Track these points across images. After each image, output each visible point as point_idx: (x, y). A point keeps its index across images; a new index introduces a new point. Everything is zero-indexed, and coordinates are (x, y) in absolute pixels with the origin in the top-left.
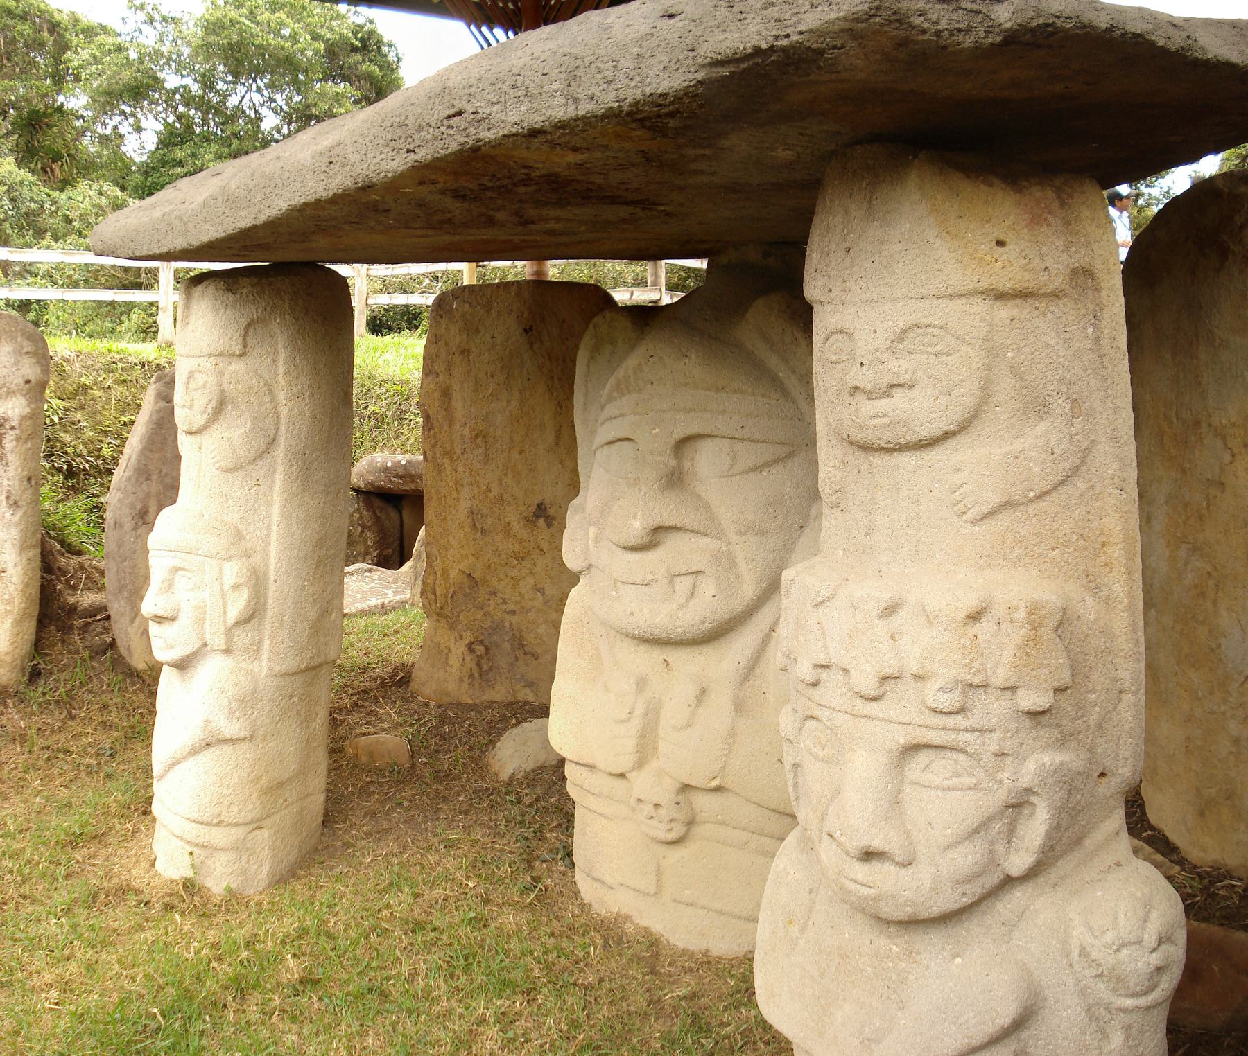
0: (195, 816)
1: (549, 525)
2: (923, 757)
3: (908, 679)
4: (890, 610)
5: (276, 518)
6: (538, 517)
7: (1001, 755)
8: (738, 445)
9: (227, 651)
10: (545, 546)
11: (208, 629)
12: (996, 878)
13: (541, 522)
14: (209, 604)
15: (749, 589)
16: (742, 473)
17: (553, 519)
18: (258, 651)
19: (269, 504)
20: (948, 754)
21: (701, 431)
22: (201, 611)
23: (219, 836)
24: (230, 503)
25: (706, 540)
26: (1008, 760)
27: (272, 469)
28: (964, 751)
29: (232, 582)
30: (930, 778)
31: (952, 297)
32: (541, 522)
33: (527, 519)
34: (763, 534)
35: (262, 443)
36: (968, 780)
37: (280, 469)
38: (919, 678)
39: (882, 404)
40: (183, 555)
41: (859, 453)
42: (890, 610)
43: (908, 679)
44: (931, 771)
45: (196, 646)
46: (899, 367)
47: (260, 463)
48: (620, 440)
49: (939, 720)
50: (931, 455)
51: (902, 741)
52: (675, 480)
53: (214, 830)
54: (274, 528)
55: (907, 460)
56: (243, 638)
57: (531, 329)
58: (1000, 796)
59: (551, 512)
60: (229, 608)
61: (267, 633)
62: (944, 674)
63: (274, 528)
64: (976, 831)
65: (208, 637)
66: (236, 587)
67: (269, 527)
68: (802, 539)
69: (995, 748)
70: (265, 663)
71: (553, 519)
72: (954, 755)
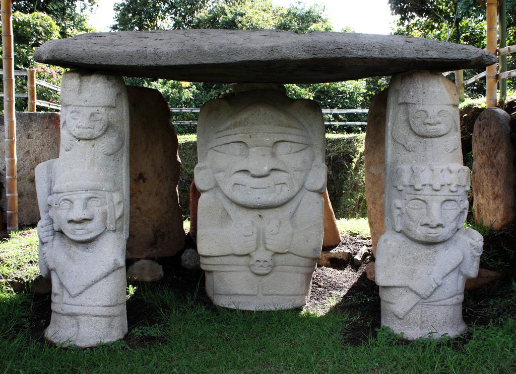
0: (109, 303)
1: (144, 182)
2: (446, 203)
3: (446, 186)
4: (442, 171)
5: (124, 174)
6: (139, 179)
7: (461, 201)
8: (292, 144)
9: (115, 231)
10: (142, 190)
11: (108, 221)
12: (456, 229)
13: (141, 181)
14: (108, 211)
15: (296, 189)
16: (293, 153)
17: (146, 179)
18: (122, 229)
19: (122, 168)
20: (451, 202)
21: (283, 140)
22: (105, 216)
23: (115, 311)
24: (109, 169)
25: (283, 174)
26: (462, 202)
27: (122, 155)
28: (455, 201)
29: (118, 201)
30: (447, 208)
31: (449, 105)
32: (141, 181)
33: (135, 180)
34: (302, 171)
35: (121, 143)
36: (455, 207)
37: (125, 154)
38: (449, 185)
39: (434, 127)
40: (95, 191)
41: (421, 139)
42: (442, 171)
43: (446, 186)
44: (449, 205)
45: (103, 230)
46: (439, 119)
47: (119, 152)
48: (234, 142)
49: (452, 194)
50: (440, 138)
51: (444, 200)
52: (274, 155)
53: (114, 308)
54: (124, 178)
55: (436, 140)
56: (119, 224)
57: (135, 104)
58: (460, 210)
59: (145, 176)
60: (116, 211)
61: (124, 222)
62: (455, 183)
63: (124, 178)
64: (456, 218)
65: (108, 225)
66: (119, 203)
67: (122, 179)
68: (310, 173)
69: (461, 199)
70: (124, 234)
71: (146, 179)
72: (452, 202)
